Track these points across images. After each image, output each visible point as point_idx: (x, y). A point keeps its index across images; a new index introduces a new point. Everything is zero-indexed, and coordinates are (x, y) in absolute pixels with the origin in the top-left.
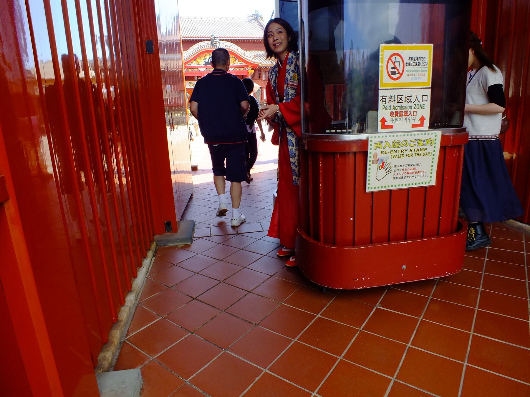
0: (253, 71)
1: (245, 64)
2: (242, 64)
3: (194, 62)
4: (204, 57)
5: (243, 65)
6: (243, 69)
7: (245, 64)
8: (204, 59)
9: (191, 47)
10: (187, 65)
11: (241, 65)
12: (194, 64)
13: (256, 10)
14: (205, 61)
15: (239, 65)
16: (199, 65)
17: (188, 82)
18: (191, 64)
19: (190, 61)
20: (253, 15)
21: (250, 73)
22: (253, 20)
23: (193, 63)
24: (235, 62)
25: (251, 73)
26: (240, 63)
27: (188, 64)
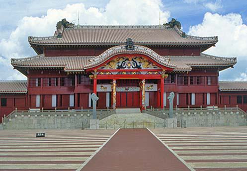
0: (167, 75)
1: (158, 68)
7: (158, 68)
9: (105, 51)
10: (100, 68)
12: (107, 68)
13: (172, 19)
15: (153, 69)
17: (100, 85)
19: (103, 64)
20: (169, 23)
21: (163, 77)
22: (169, 27)
24: (149, 66)
25: (165, 77)
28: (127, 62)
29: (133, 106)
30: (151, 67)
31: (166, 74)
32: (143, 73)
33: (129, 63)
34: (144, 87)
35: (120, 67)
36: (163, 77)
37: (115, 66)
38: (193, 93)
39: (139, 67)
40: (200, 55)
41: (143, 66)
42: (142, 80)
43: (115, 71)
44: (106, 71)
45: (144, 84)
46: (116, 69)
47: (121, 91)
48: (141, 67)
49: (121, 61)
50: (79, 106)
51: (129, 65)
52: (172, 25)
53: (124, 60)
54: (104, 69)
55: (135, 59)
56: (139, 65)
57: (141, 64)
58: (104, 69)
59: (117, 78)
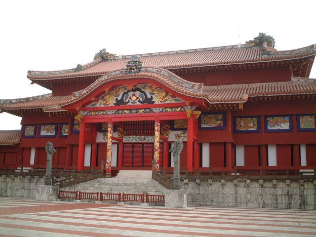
0: (200, 113)
2: (178, 100)
3: (100, 101)
4: (117, 92)
5: (180, 102)
6: (179, 109)
8: (115, 96)
11: (178, 102)
12: (100, 104)
14: (117, 99)
15: (173, 102)
16: (107, 105)
17: (103, 133)
18: (96, 104)
20: (254, 39)
21: (189, 115)
22: (254, 46)
23: (99, 103)
25: (193, 115)
26: (175, 100)
27: (91, 104)
28: (131, 94)
29: (143, 166)
30: (170, 100)
31: (197, 109)
32: (157, 110)
33: (134, 95)
34: (157, 134)
35: (119, 102)
36: (189, 115)
37: (112, 102)
38: (272, 144)
39: (149, 101)
40: (290, 80)
41: (157, 100)
42: (153, 123)
43: (111, 108)
44: (99, 110)
45: (156, 128)
46: (113, 105)
47: (134, 141)
48: (154, 100)
49: (122, 93)
50: (71, 165)
51: (134, 98)
52: (258, 41)
53: (126, 91)
54: (96, 106)
55: (144, 88)
56: (149, 96)
57: (153, 96)
58: (96, 106)
59: (113, 120)
